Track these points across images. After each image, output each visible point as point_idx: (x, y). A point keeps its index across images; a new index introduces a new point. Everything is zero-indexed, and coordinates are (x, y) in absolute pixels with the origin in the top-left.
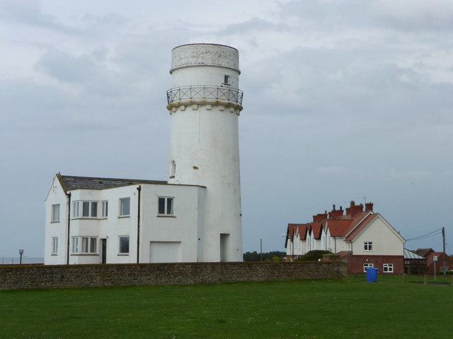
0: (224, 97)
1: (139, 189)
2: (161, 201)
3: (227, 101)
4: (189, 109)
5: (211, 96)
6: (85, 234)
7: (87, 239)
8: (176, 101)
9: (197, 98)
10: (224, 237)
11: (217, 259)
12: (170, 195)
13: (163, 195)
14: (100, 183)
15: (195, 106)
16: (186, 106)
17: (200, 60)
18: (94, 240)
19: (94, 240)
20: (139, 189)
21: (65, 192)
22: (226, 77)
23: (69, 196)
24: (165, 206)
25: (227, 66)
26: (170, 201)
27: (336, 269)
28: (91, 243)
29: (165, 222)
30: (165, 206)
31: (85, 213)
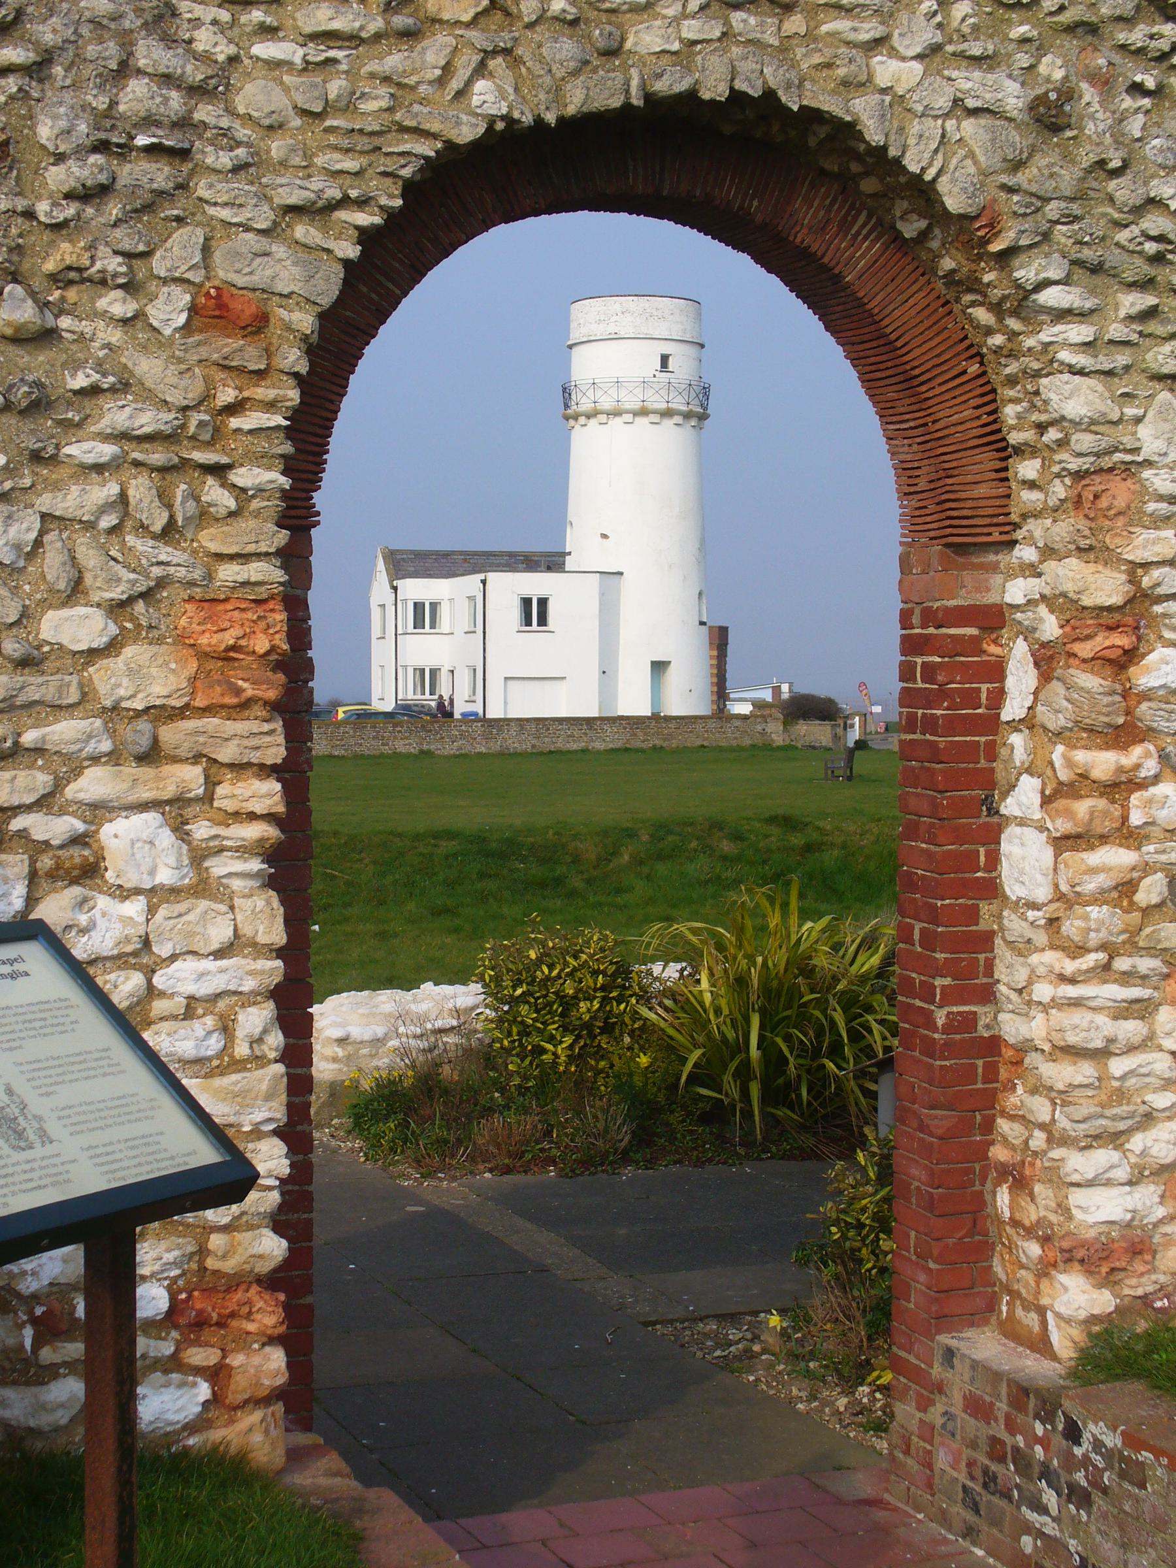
0: (656, 397)
1: (484, 582)
2: (527, 602)
3: (664, 406)
4: (593, 421)
5: (629, 397)
6: (420, 663)
7: (423, 671)
8: (585, 405)
9: (606, 404)
10: (659, 667)
11: (645, 711)
12: (543, 593)
13: (527, 592)
14: (465, 560)
15: (603, 418)
16: (588, 417)
17: (612, 329)
18: (434, 672)
19: (434, 672)
20: (484, 582)
21: (391, 582)
22: (665, 359)
23: (395, 589)
24: (535, 613)
25: (666, 335)
26: (543, 602)
27: (759, 728)
28: (428, 677)
29: (535, 639)
30: (535, 613)
31: (419, 623)
